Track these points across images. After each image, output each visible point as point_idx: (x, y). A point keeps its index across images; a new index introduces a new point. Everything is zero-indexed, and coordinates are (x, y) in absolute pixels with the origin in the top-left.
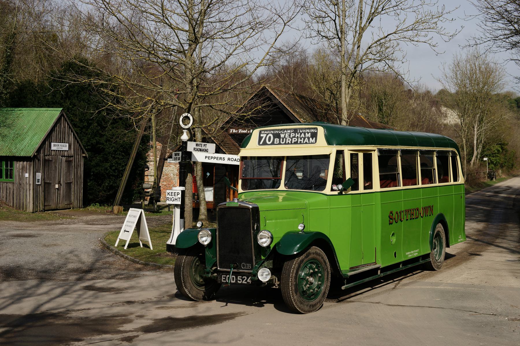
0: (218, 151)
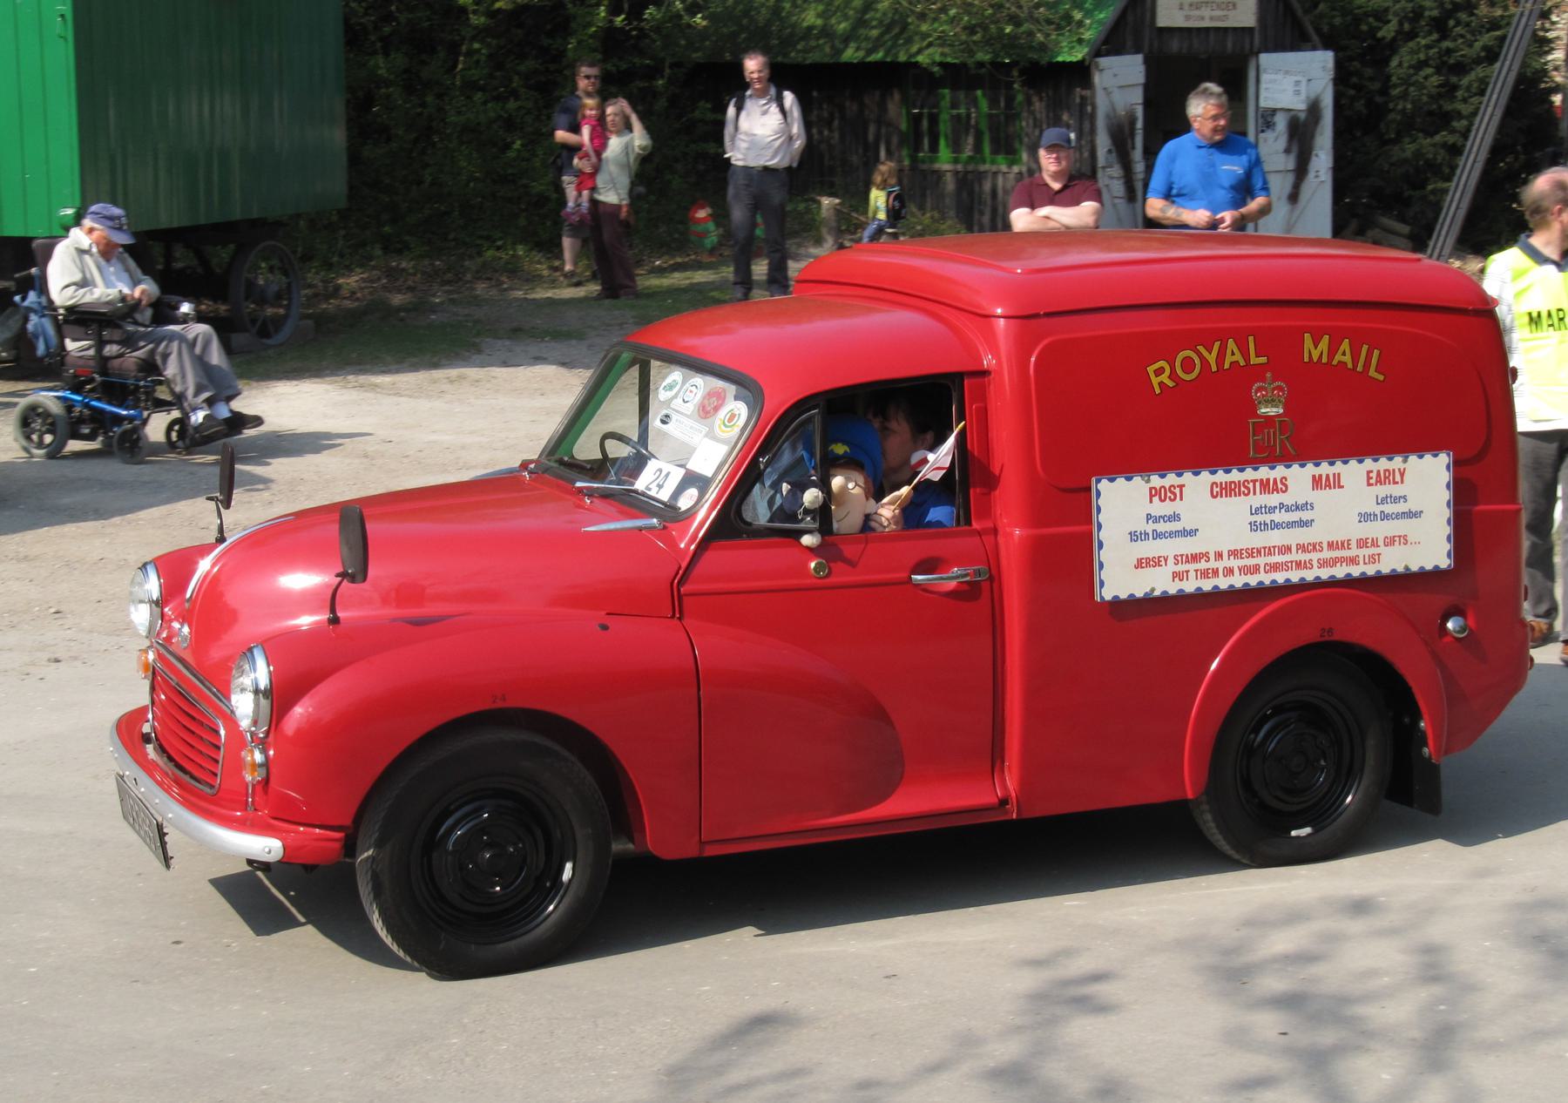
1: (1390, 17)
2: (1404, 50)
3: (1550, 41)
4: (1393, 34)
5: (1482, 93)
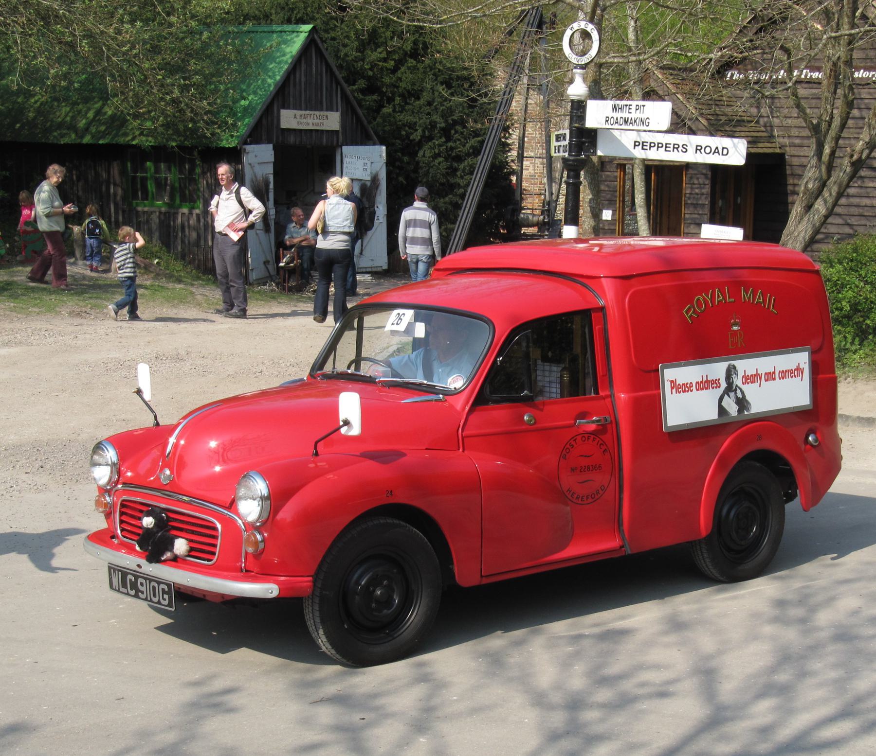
0: (679, 124)
1: (417, 128)
2: (426, 147)
3: (508, 145)
4: (419, 137)
5: (472, 173)
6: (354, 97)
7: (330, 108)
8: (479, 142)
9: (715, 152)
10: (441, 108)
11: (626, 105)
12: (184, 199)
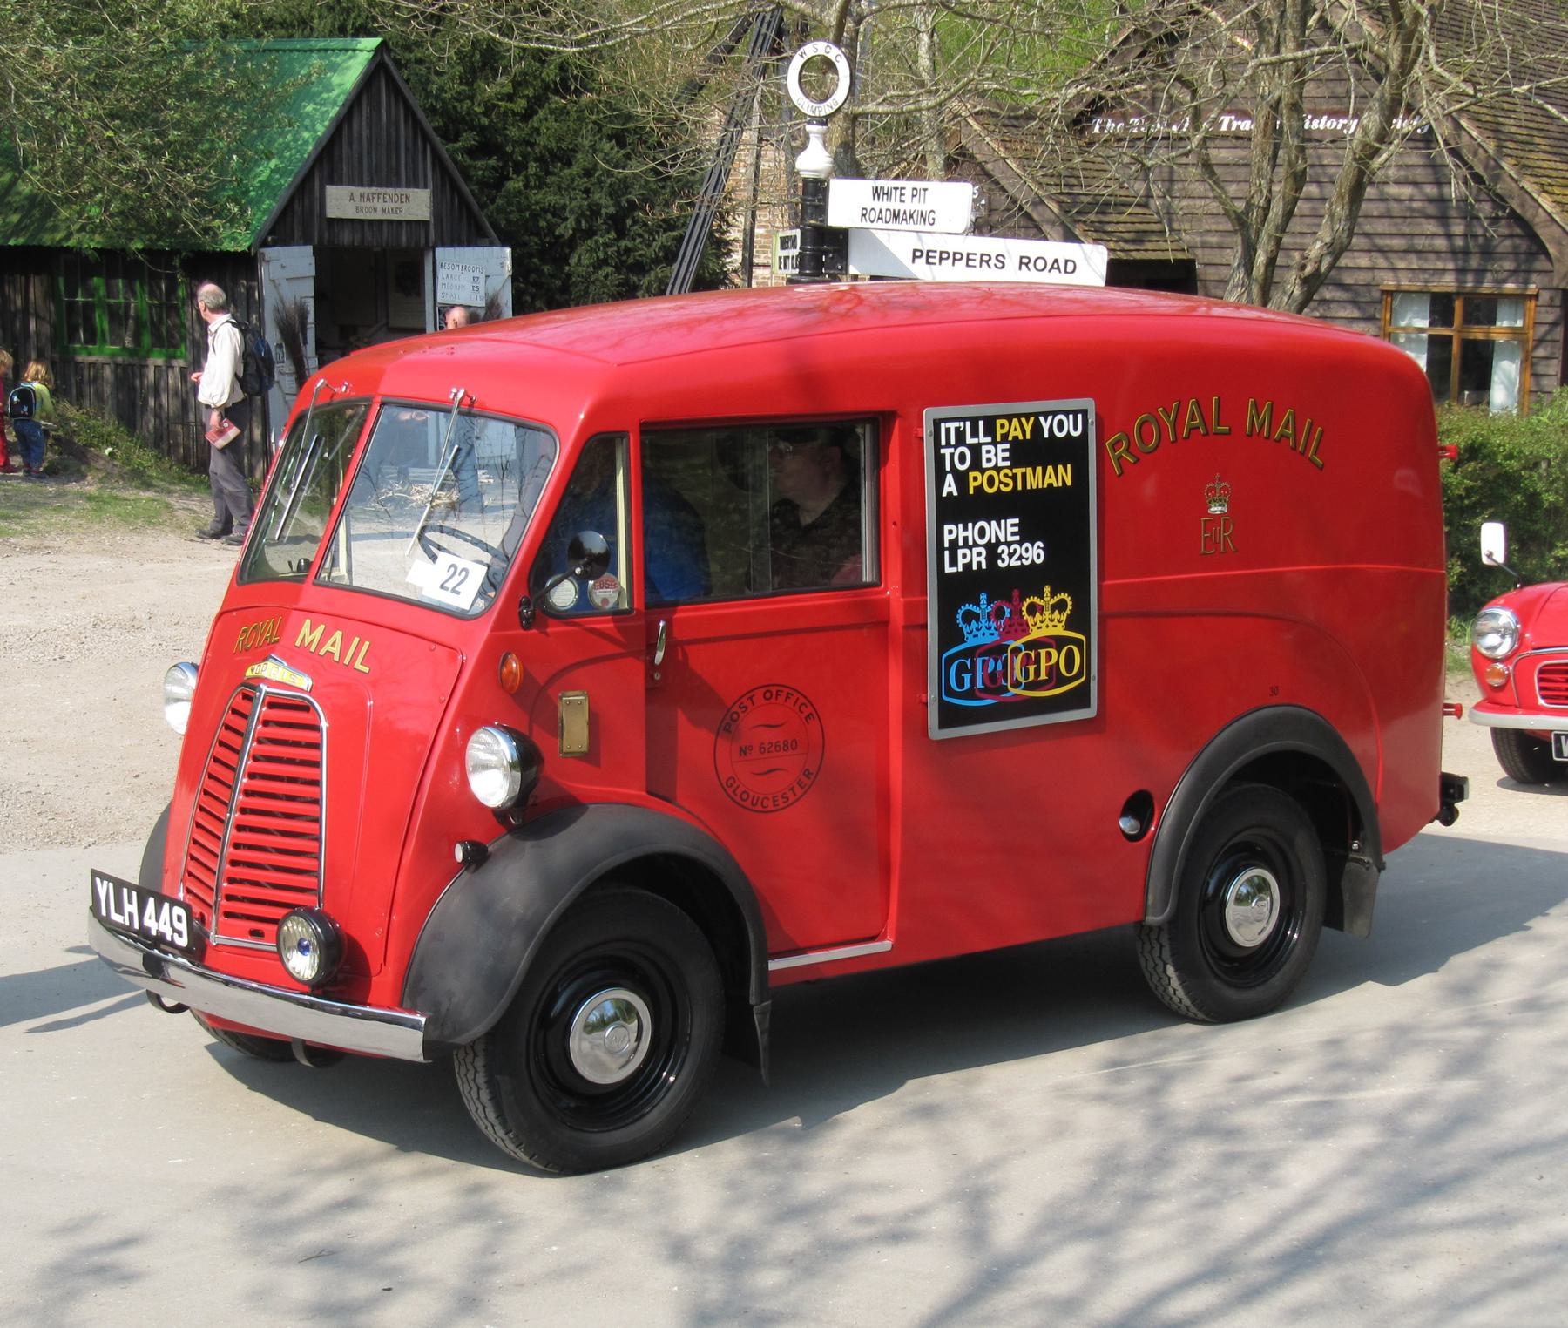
1: (567, 214)
2: (582, 249)
3: (728, 243)
4: (571, 232)
6: (456, 162)
7: (413, 183)
8: (674, 238)
9: (1052, 268)
10: (609, 181)
11: (896, 189)
12: (159, 341)
